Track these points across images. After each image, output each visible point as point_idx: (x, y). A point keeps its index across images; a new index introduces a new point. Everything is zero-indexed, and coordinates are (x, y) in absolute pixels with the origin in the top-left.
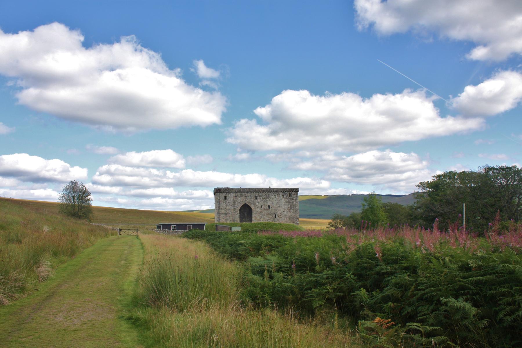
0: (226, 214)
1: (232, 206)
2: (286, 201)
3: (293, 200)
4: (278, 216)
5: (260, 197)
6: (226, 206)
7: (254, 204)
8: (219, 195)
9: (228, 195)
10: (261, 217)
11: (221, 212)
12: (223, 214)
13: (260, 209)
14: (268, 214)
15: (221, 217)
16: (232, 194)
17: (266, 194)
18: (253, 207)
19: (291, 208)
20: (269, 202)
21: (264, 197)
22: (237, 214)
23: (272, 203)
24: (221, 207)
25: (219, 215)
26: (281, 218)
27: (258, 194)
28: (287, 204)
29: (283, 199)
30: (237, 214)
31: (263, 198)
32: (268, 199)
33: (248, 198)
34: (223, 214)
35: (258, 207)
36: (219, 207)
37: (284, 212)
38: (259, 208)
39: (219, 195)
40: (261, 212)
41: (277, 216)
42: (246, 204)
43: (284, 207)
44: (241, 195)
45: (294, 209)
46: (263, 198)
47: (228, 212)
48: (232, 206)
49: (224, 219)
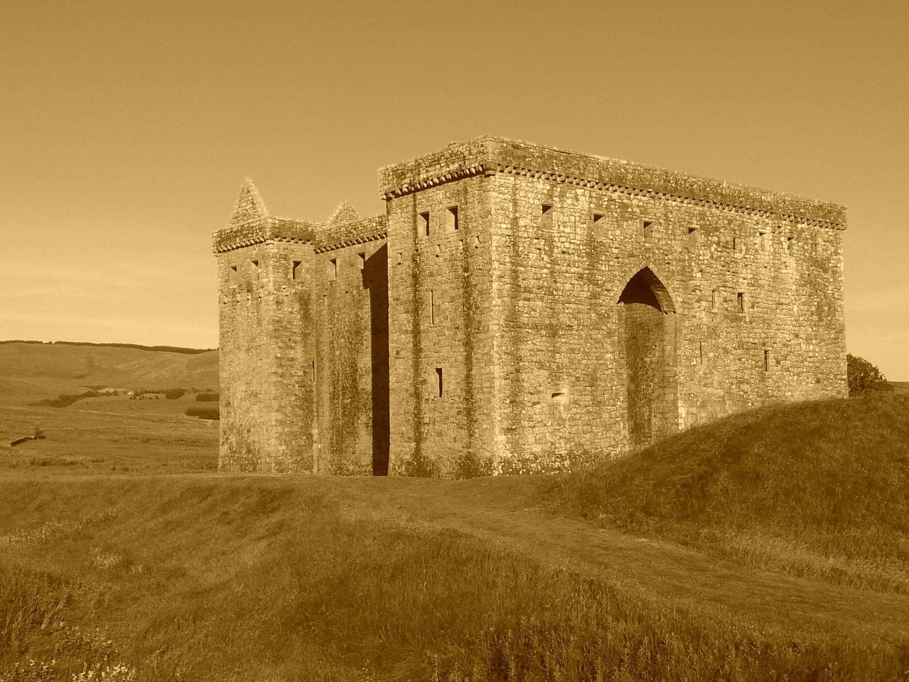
0: (553, 332)
1: (581, 277)
2: (802, 276)
3: (826, 271)
4: (778, 363)
5: (707, 234)
6: (552, 272)
7: (686, 275)
8: (515, 189)
9: (562, 196)
10: (715, 367)
11: (524, 319)
12: (536, 327)
13: (709, 311)
14: (741, 345)
15: (525, 349)
16: (580, 192)
17: (730, 221)
18: (678, 298)
19: (820, 320)
20: (744, 271)
21: (723, 239)
22: (610, 334)
23: (754, 283)
24: (528, 279)
25: (517, 341)
26: (788, 377)
27: (702, 216)
28: (807, 290)
29: (792, 262)
30: (610, 334)
31: (718, 244)
32: (737, 255)
33: (658, 232)
34: (536, 327)
35: (698, 301)
36: (515, 274)
37: (797, 336)
38: (704, 304)
39: (515, 189)
40: (713, 332)
41: (771, 362)
42: (647, 269)
43: (795, 309)
44: (624, 207)
45: (829, 327)
46: (718, 244)
47: (564, 319)
48: (581, 277)
49: (541, 366)
